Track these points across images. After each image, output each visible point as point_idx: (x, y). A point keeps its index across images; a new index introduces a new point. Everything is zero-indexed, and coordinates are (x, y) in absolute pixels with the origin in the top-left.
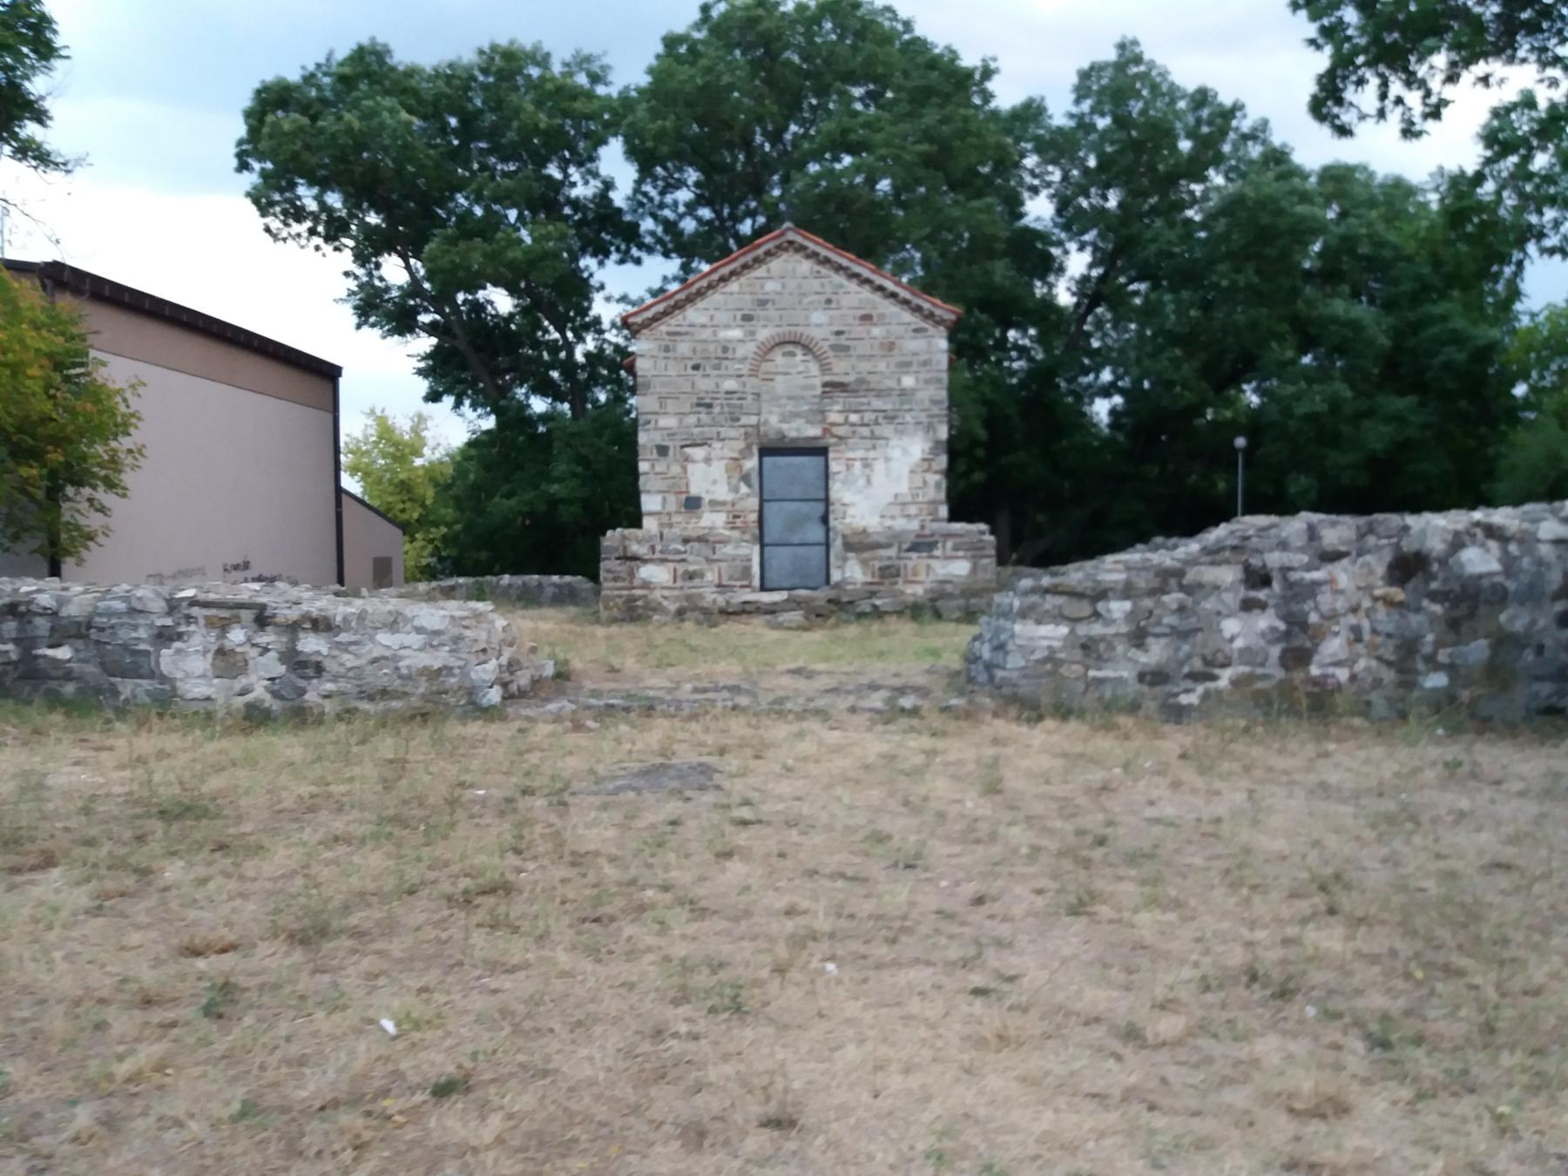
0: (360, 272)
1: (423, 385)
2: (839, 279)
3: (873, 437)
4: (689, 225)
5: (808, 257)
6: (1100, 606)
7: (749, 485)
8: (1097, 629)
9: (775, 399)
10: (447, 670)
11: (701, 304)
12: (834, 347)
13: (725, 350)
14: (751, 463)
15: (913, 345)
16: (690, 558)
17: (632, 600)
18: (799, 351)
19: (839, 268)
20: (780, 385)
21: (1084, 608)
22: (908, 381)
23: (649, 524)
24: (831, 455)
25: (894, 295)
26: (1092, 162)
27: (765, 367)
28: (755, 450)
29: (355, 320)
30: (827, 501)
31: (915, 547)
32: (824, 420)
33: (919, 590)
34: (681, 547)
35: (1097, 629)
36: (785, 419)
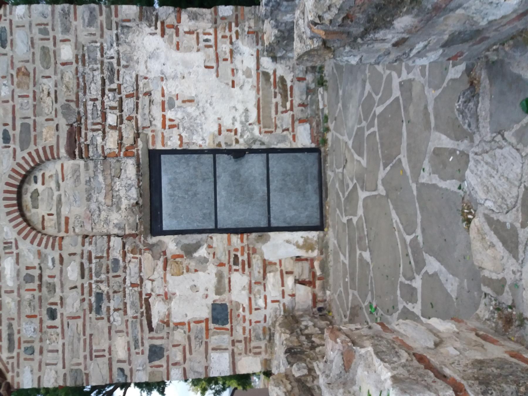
3: (135, 95)
7: (197, 246)
13: (29, 279)
14: (171, 244)
18: (31, 187)
20: (73, 210)
22: (67, 52)
24: (159, 147)
27: (51, 230)
30: (214, 152)
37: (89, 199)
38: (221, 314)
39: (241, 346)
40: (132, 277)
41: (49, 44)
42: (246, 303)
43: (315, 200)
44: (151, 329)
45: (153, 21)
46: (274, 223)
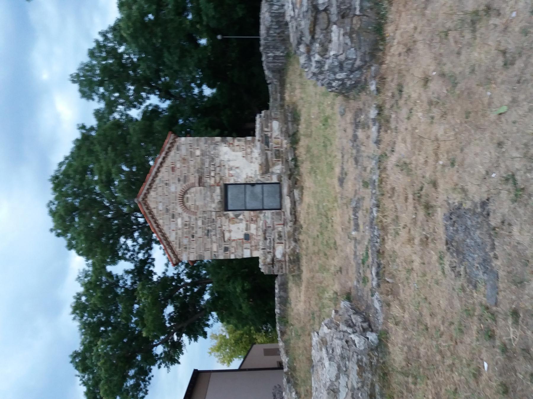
0: (159, 362)
1: (200, 338)
2: (157, 180)
4: (140, 241)
5: (149, 193)
6: (321, 8)
7: (239, 215)
8: (334, 10)
9: (205, 205)
10: (359, 362)
11: (168, 235)
12: (185, 182)
14: (231, 214)
15: (183, 151)
16: (273, 237)
17: (290, 261)
18: (187, 196)
19: (153, 181)
21: (322, 17)
22: (198, 153)
23: (255, 254)
25: (164, 158)
26: (117, 95)
28: (226, 213)
29: (176, 365)
31: (267, 144)
32: (213, 186)
33: (285, 142)
34: (268, 241)
35: (334, 10)
36: (213, 202)
37: (205, 200)
38: (247, 237)
39: (254, 248)
40: (218, 225)
41: (192, 150)
42: (255, 233)
43: (278, 199)
44: (225, 242)
45: (225, 142)
46: (265, 208)
